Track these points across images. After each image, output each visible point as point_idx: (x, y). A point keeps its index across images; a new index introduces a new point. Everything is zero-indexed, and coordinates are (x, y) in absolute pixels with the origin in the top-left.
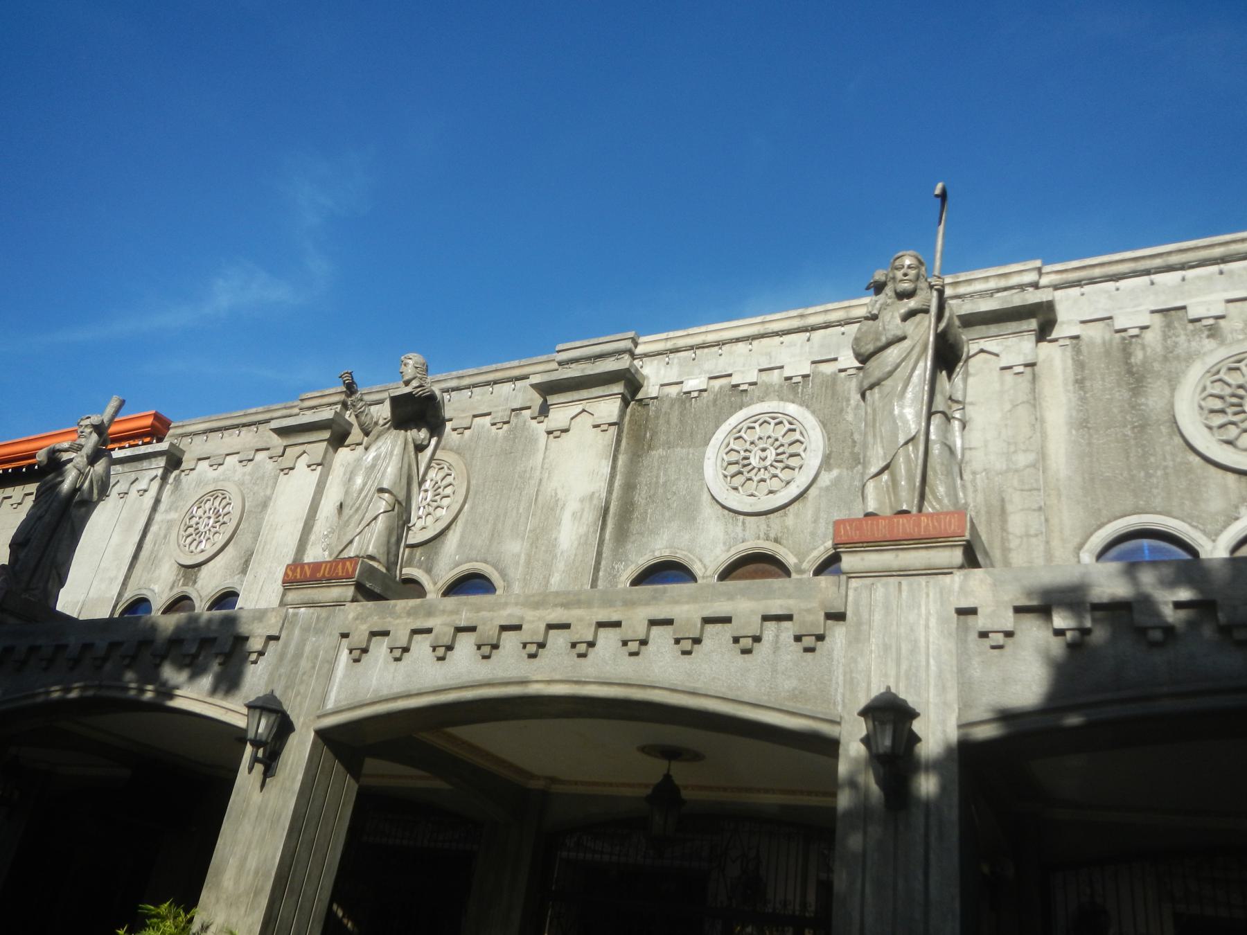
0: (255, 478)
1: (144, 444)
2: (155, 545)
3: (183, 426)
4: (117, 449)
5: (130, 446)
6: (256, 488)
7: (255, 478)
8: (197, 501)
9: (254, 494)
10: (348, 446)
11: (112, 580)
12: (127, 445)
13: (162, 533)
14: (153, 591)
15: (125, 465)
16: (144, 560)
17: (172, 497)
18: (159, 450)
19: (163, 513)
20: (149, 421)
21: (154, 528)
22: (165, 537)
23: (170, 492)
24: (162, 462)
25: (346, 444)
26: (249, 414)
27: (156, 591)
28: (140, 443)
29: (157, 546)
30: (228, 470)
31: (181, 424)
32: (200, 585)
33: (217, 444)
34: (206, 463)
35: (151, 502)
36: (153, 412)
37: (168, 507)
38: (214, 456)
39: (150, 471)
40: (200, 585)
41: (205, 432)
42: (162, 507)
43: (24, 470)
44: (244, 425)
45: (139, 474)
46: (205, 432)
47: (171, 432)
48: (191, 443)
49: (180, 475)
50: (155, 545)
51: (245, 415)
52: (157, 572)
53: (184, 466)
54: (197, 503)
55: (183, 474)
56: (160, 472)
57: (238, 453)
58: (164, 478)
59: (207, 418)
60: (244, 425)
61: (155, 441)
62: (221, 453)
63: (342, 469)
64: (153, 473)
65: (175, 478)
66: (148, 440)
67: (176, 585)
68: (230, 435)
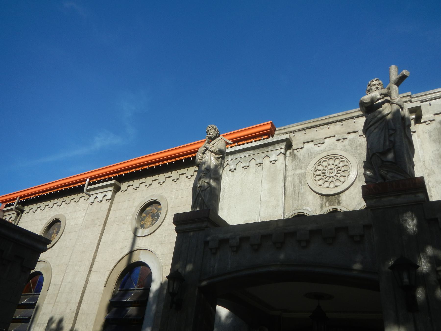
0: (354, 146)
1: (264, 139)
2: (295, 187)
3: (284, 129)
4: (246, 143)
5: (255, 141)
6: (359, 152)
7: (354, 146)
8: (317, 162)
9: (359, 154)
10: (424, 122)
11: (275, 207)
12: (253, 141)
13: (297, 180)
14: (307, 210)
15: (256, 150)
16: (291, 195)
17: (294, 162)
18: (282, 139)
19: (291, 171)
20: (269, 127)
21: (289, 179)
22: (300, 182)
23: (291, 161)
24: (283, 145)
25: (422, 121)
26: (331, 117)
27: (310, 210)
28: (262, 138)
29: (296, 187)
30: (330, 145)
31: (283, 128)
32: (345, 204)
33: (311, 134)
34: (311, 144)
35: (283, 166)
36: (271, 122)
37: (294, 168)
38: (316, 140)
39: (275, 151)
40: (345, 204)
41: (303, 129)
42: (289, 168)
43: (183, 161)
44: (331, 123)
45: (268, 154)
46: (303, 129)
47: (276, 133)
48: (294, 136)
49: (293, 152)
50: (295, 187)
51: (329, 118)
52: (305, 201)
53: (294, 147)
54: (317, 163)
55: (295, 151)
56: (283, 151)
57: (334, 136)
58: (285, 154)
59: (301, 123)
60: (331, 123)
61: (271, 137)
62: (322, 137)
63: (427, 135)
64: (279, 152)
65: (290, 153)
66: (266, 137)
67: (324, 205)
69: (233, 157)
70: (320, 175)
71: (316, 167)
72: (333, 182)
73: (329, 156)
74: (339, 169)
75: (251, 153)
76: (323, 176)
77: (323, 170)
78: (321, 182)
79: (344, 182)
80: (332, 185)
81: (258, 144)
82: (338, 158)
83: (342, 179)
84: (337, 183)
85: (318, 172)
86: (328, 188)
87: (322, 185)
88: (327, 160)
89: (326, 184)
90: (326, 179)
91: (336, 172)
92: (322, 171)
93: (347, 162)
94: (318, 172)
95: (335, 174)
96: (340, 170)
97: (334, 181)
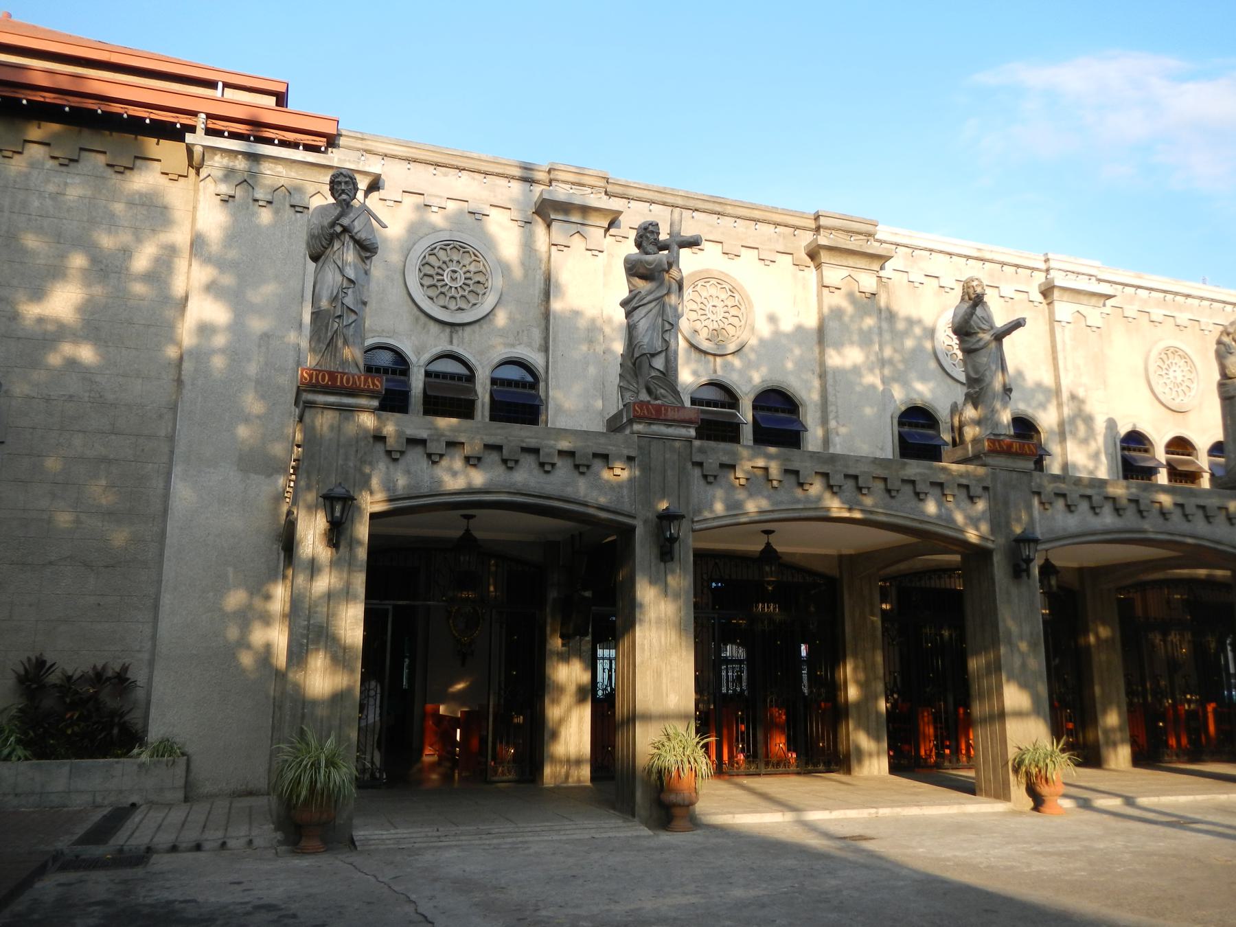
68: (446, 175)
69: (227, 161)
70: (431, 276)
71: (425, 257)
72: (455, 298)
73: (452, 242)
74: (468, 275)
75: (279, 172)
76: (438, 280)
77: (439, 268)
78: (432, 292)
79: (475, 304)
80: (453, 306)
81: (304, 158)
82: (468, 252)
83: (472, 299)
84: (463, 305)
85: (428, 270)
86: (444, 307)
87: (435, 299)
88: (448, 248)
89: (442, 301)
90: (443, 290)
91: (463, 280)
92: (436, 268)
93: (484, 265)
94: (428, 270)
95: (456, 286)
96: (470, 279)
97: (458, 299)
